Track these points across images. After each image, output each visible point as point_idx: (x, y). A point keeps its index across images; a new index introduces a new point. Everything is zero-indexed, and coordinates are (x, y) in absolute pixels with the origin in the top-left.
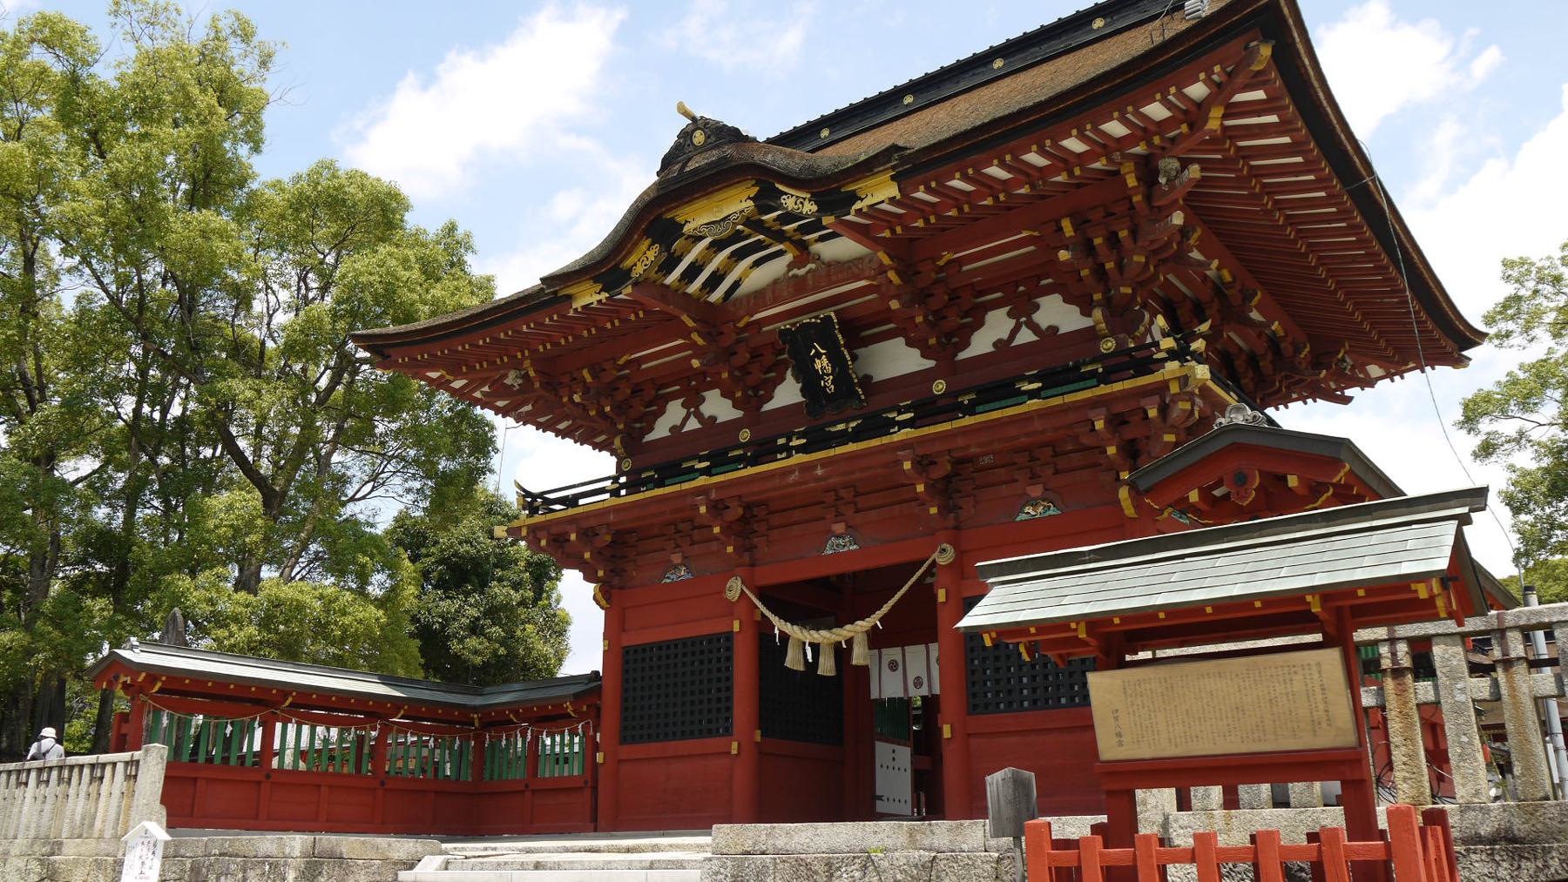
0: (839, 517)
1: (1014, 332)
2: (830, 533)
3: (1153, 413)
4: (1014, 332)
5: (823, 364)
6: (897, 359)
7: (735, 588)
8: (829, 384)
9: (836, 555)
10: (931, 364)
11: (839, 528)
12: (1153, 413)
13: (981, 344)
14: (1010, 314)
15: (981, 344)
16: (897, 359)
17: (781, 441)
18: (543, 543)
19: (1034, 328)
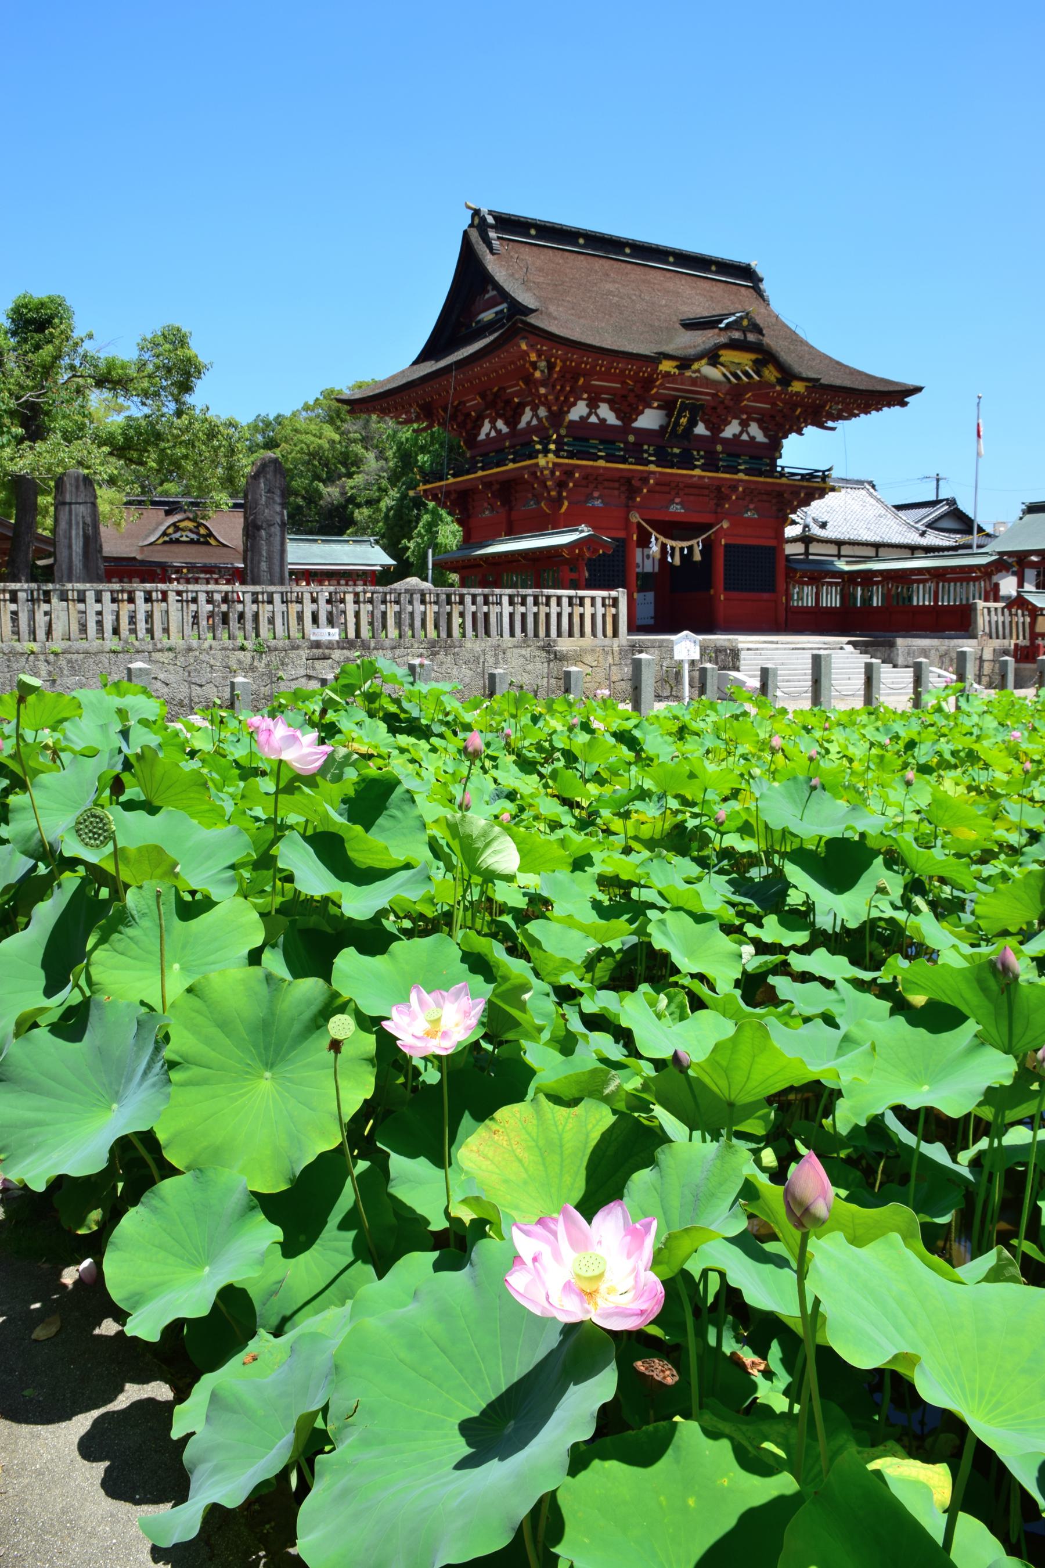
2: (672, 502)
5: (683, 421)
8: (680, 429)
9: (675, 513)
17: (646, 447)
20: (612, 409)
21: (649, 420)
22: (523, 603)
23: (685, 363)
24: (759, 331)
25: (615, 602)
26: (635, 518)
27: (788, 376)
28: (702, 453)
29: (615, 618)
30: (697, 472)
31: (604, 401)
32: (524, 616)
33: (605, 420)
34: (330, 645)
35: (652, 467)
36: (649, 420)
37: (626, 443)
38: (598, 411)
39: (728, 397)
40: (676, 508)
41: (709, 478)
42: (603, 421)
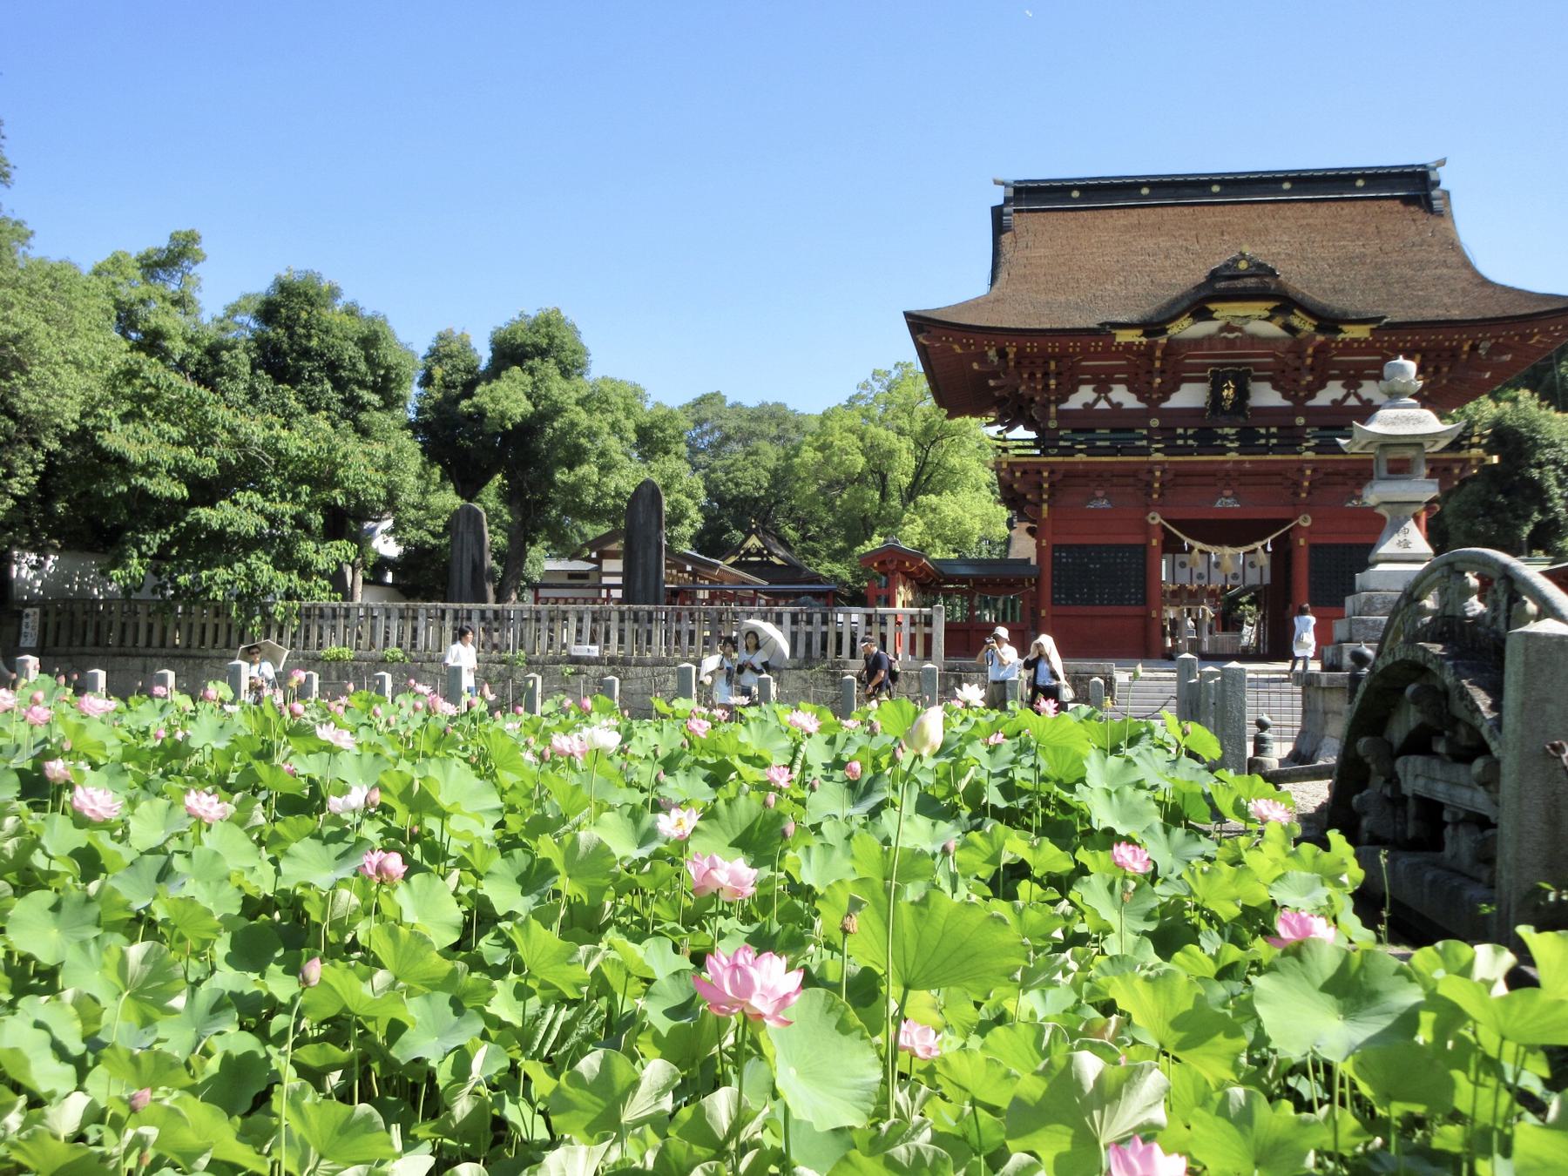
0: (1228, 486)
1: (1346, 397)
2: (1221, 495)
3: (1457, 471)
4: (1346, 397)
6: (1266, 396)
7: (1156, 519)
10: (1287, 403)
11: (1228, 492)
12: (1457, 471)
13: (1323, 398)
14: (1344, 386)
15: (1323, 398)
16: (1266, 396)
17: (1180, 431)
18: (1018, 474)
19: (1358, 397)
20: (1130, 390)
21: (1190, 396)
22: (809, 622)
23: (1152, 327)
24: (1272, 272)
25: (928, 622)
26: (1156, 519)
27: (1329, 322)
28: (1273, 430)
29: (928, 639)
30: (1233, 456)
31: (1119, 381)
32: (809, 635)
33: (1120, 404)
34: (589, 661)
35: (1159, 457)
36: (1190, 396)
37: (1149, 428)
38: (1111, 395)
39: (1290, 356)
40: (1227, 503)
41: (1251, 462)
42: (1117, 407)
